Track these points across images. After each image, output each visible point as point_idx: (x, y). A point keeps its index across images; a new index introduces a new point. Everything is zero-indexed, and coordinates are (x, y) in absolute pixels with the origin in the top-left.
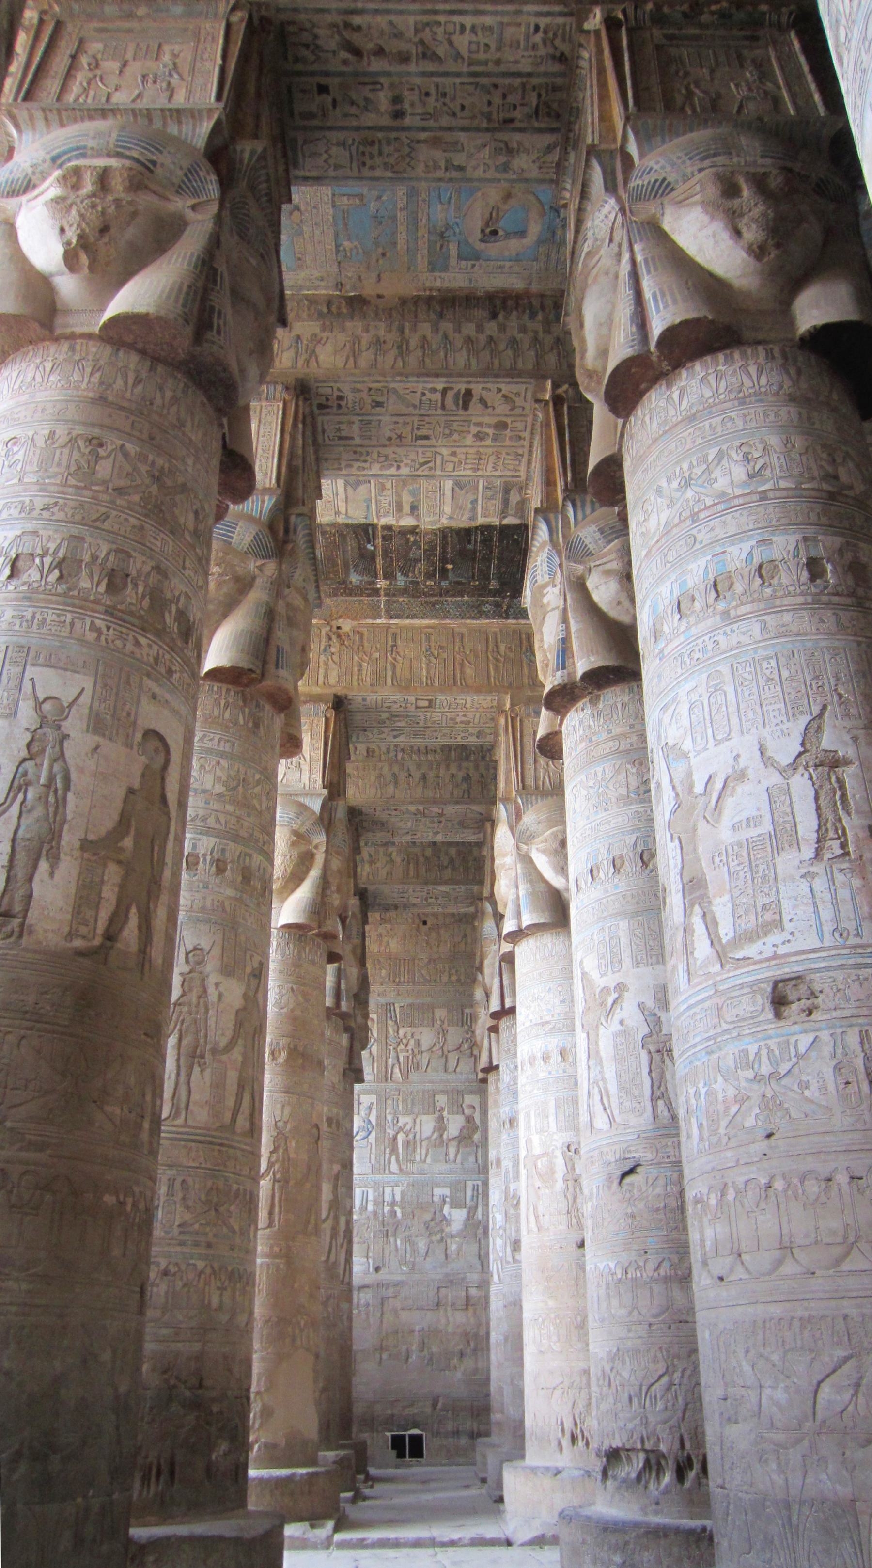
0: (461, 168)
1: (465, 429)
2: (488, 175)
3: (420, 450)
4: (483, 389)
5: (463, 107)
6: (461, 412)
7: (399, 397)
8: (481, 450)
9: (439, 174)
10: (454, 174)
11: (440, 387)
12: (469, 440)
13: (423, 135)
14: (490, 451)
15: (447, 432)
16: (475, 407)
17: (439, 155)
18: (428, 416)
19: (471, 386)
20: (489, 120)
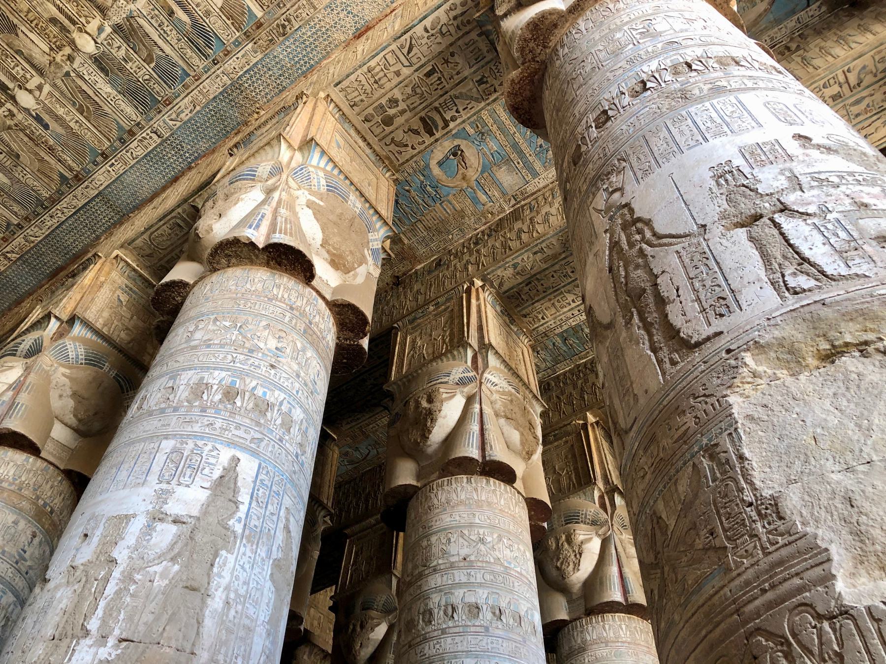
0: (535, 253)
1: (409, 102)
2: (520, 258)
3: (424, 60)
4: (424, 142)
5: (553, 276)
6: (423, 114)
7: (471, 98)
8: (383, 91)
9: (544, 245)
10: (536, 249)
11: (452, 125)
12: (397, 94)
13: (563, 256)
14: (376, 95)
15: (418, 90)
16: (417, 124)
17: (549, 252)
18: (441, 96)
19: (432, 139)
20: (537, 279)
